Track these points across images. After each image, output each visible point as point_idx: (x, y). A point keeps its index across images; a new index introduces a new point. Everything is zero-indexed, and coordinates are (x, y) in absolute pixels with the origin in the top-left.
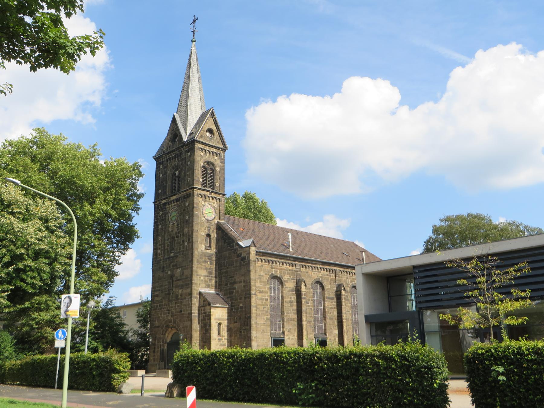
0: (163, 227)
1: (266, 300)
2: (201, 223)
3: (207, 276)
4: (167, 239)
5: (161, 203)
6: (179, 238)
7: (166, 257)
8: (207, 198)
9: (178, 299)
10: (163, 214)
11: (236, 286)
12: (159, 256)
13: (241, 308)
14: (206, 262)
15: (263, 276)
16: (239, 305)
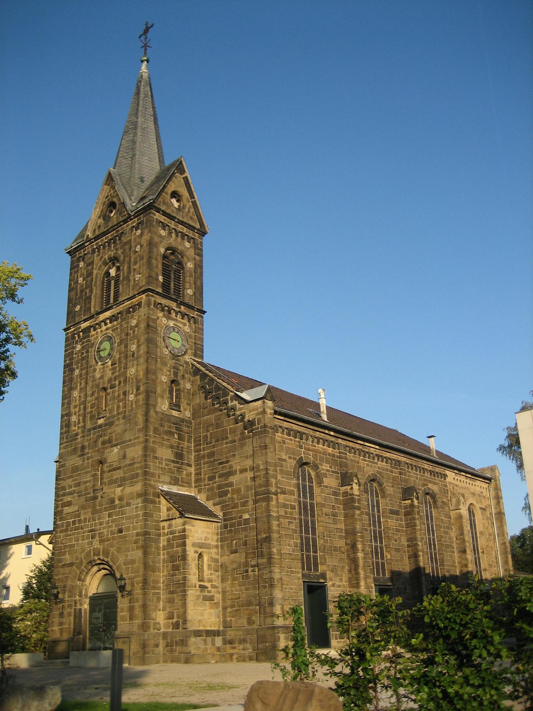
0: (84, 372)
1: (293, 507)
2: (162, 358)
3: (174, 462)
4: (89, 393)
5: (80, 327)
6: (117, 388)
7: (89, 425)
8: (173, 315)
9: (114, 507)
10: (83, 348)
11: (233, 479)
12: (73, 428)
13: (247, 521)
14: (171, 433)
15: (285, 460)
16: (241, 517)
